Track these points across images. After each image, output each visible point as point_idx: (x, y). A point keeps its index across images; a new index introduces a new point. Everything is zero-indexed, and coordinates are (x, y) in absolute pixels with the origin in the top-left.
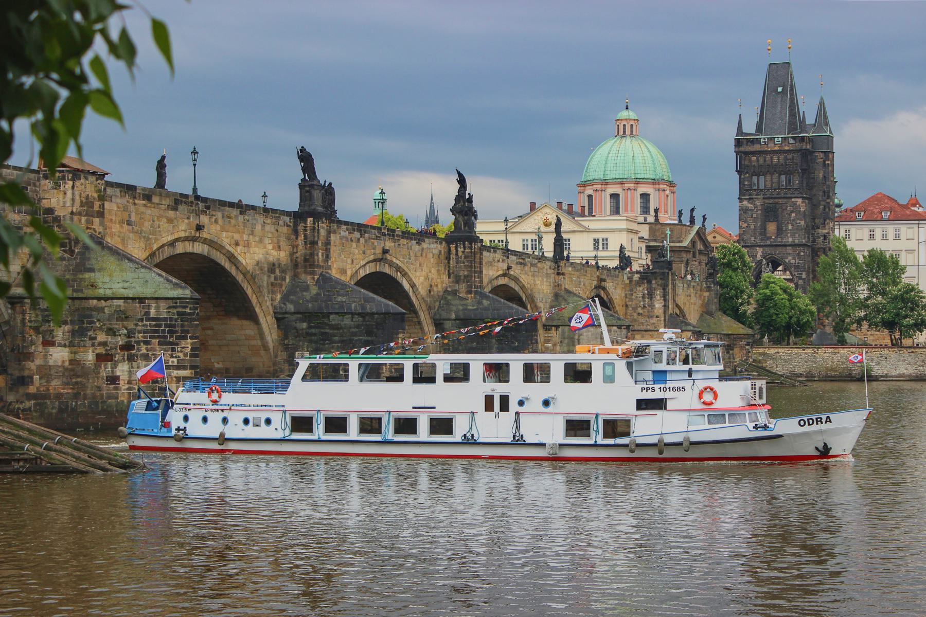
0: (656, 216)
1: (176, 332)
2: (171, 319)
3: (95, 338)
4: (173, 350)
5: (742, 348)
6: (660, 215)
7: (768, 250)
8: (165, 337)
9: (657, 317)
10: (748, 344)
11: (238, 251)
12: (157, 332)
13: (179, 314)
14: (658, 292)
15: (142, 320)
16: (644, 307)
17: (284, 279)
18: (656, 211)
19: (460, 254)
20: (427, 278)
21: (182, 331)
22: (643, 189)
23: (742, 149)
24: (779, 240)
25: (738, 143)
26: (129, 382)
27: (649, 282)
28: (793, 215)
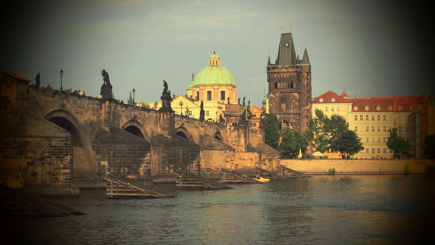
0: (228, 101)
1: (63, 152)
2: (61, 146)
3: (27, 155)
4: (62, 160)
5: (276, 160)
6: (230, 101)
7: (281, 116)
8: (59, 155)
9: (242, 146)
10: (279, 158)
11: (78, 117)
12: (54, 152)
13: (64, 144)
14: (242, 135)
15: (48, 147)
16: (236, 141)
17: (96, 129)
18: (228, 99)
19: (165, 117)
20: (151, 129)
21: (66, 152)
22: (222, 89)
23: (270, 71)
24: (287, 111)
25: (268, 69)
26: (42, 175)
27: (238, 130)
28: (294, 100)
